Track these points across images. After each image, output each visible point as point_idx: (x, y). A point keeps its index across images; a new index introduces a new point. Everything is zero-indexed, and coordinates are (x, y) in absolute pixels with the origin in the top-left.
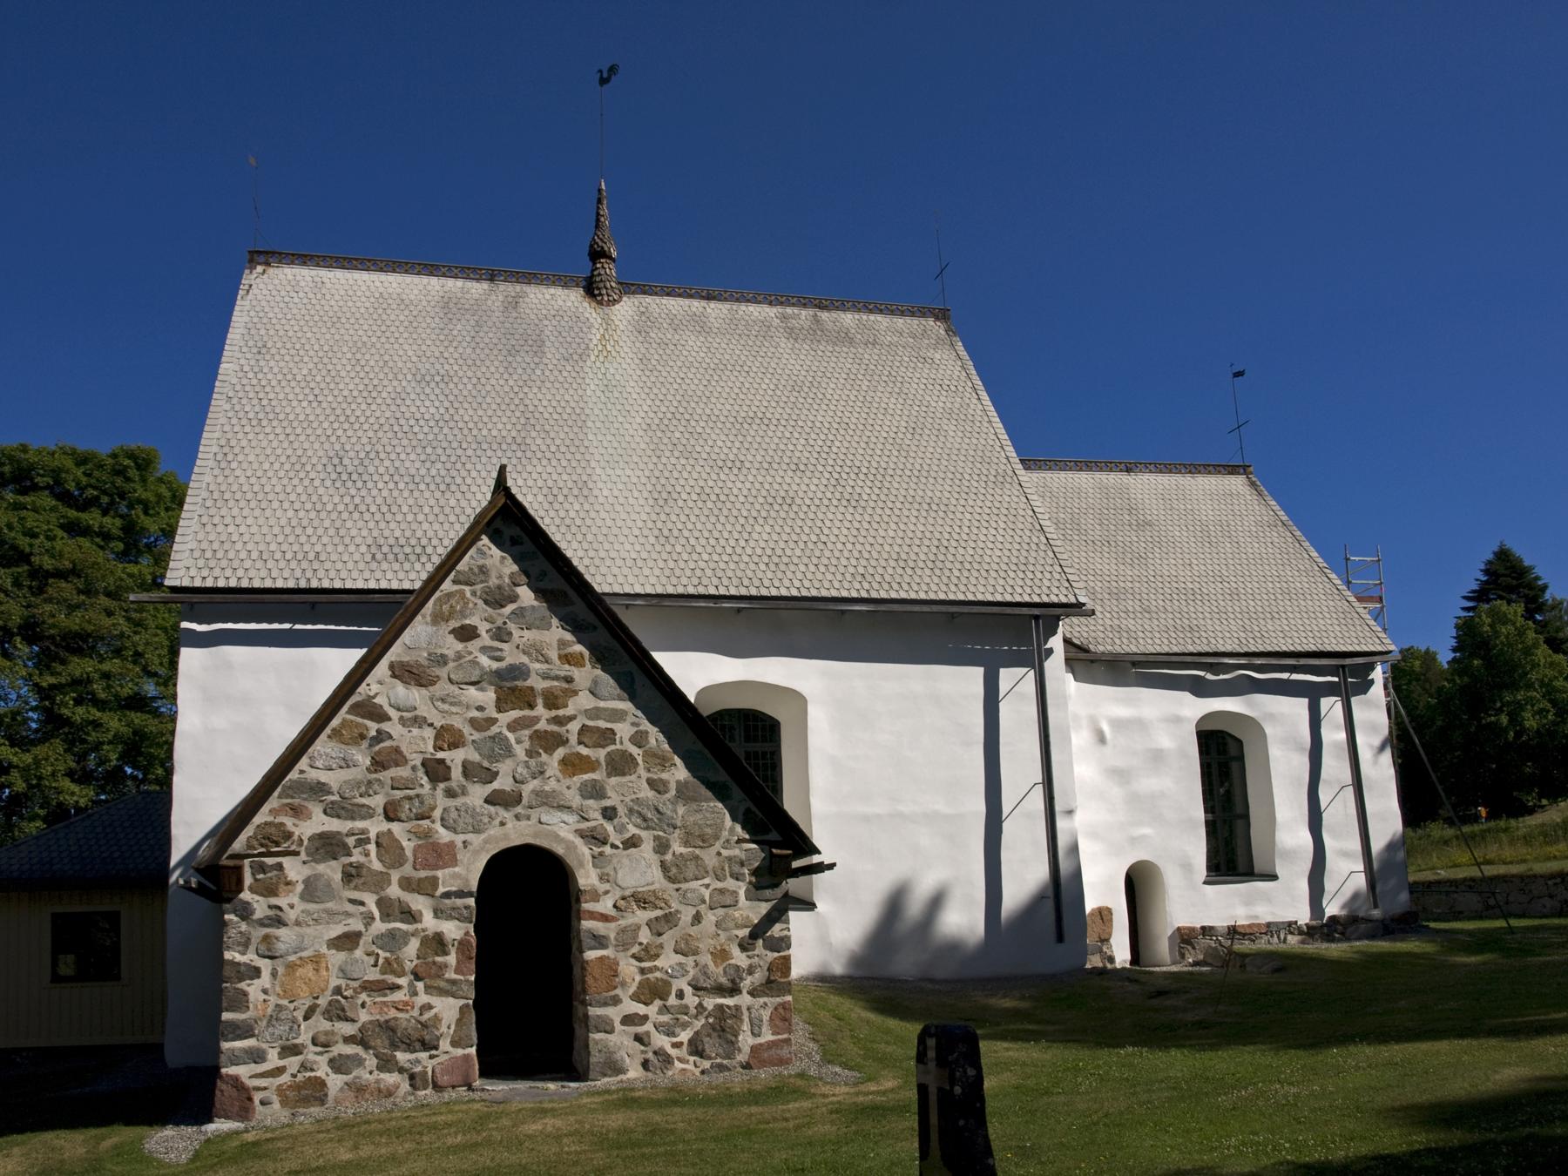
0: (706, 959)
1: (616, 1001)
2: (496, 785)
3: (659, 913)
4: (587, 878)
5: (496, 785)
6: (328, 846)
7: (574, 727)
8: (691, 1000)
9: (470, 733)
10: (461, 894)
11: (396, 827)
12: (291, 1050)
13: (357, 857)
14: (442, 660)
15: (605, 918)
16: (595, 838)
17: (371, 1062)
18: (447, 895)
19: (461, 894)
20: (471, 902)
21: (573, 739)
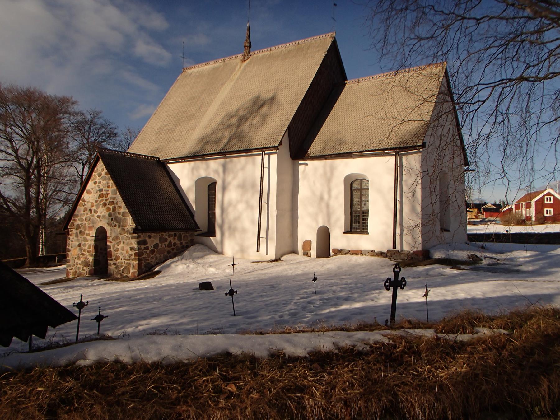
0: (125, 252)
1: (112, 260)
2: (98, 214)
3: (118, 241)
4: (108, 234)
5: (98, 214)
6: (78, 227)
7: (108, 201)
8: (123, 261)
9: (95, 204)
10: (92, 236)
11: (87, 223)
12: (74, 265)
13: (81, 229)
14: (92, 189)
15: (111, 242)
16: (109, 224)
17: (82, 269)
18: (91, 237)
19: (92, 236)
20: (94, 238)
21: (108, 204)
